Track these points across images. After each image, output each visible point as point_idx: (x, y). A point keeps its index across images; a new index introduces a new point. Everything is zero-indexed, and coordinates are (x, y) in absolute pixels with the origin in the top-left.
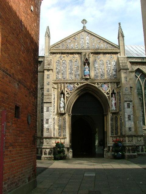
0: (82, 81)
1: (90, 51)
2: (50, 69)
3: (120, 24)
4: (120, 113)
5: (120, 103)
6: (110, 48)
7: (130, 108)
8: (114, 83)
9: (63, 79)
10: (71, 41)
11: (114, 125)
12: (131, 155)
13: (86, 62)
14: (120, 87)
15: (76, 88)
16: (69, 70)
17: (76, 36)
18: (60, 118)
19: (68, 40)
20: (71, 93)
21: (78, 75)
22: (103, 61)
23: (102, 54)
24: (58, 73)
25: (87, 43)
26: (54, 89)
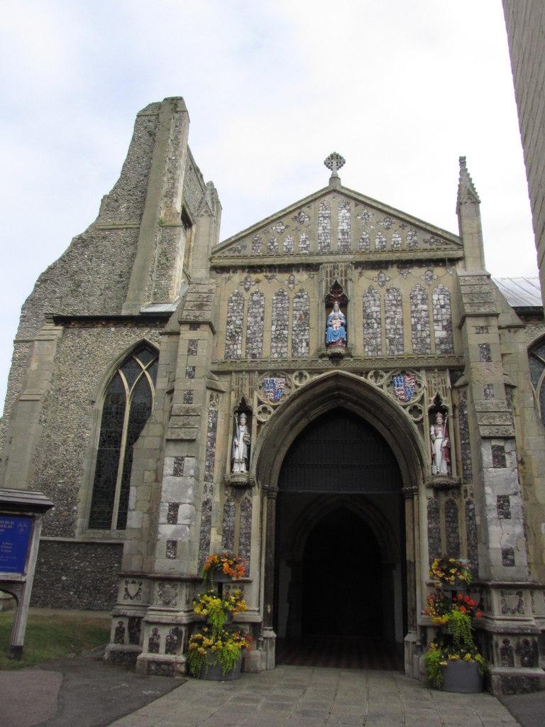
0: (322, 363)
1: (351, 257)
2: (201, 319)
3: (462, 161)
4: (468, 486)
5: (466, 446)
6: (427, 246)
7: (504, 466)
8: (442, 369)
9: (249, 357)
10: (287, 227)
13: (336, 297)
14: (466, 385)
15: (294, 391)
16: (274, 328)
17: (303, 209)
18: (232, 504)
19: (274, 224)
20: (275, 408)
21: (304, 344)
22: (397, 290)
23: (395, 266)
24: (233, 337)
25: (343, 233)
26: (215, 394)
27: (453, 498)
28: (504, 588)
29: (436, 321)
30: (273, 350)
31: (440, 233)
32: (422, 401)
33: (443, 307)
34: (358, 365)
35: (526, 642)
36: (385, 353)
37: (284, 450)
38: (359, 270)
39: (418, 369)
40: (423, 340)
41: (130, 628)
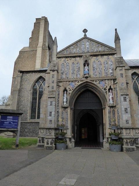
0: (84, 79)
2: (55, 69)
3: (116, 30)
7: (126, 101)
8: (111, 79)
11: (112, 117)
12: (129, 148)
13: (86, 63)
15: (77, 86)
24: (62, 73)
25: (88, 48)
26: (59, 87)
28: (126, 129)
29: (110, 68)
30: (72, 76)
31: (111, 47)
32: (106, 87)
33: (111, 65)
34: (92, 79)
35: (131, 141)
36: (98, 76)
37: (75, 99)
38: (92, 57)
39: (106, 80)
40: (107, 73)
41: (42, 140)
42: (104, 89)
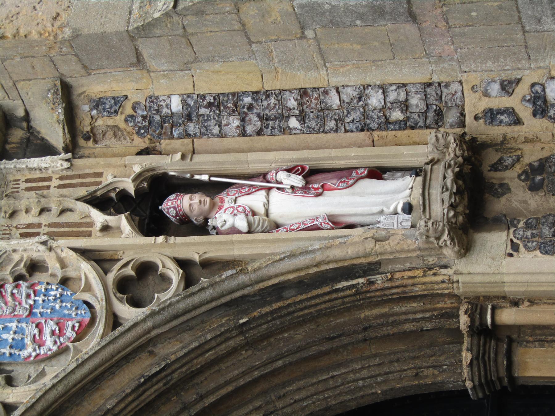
27: (518, 169)
42: (136, 303)
